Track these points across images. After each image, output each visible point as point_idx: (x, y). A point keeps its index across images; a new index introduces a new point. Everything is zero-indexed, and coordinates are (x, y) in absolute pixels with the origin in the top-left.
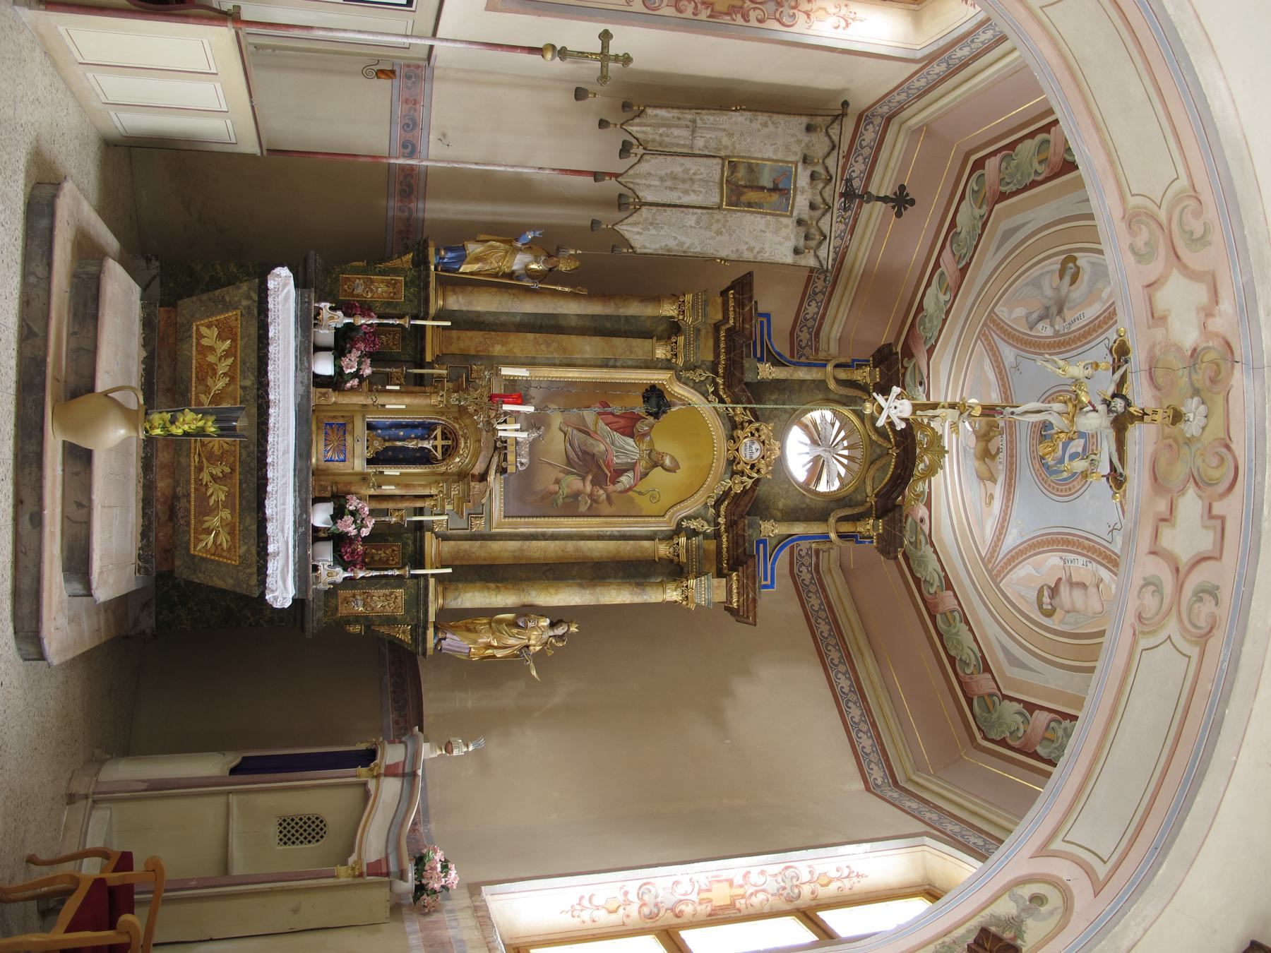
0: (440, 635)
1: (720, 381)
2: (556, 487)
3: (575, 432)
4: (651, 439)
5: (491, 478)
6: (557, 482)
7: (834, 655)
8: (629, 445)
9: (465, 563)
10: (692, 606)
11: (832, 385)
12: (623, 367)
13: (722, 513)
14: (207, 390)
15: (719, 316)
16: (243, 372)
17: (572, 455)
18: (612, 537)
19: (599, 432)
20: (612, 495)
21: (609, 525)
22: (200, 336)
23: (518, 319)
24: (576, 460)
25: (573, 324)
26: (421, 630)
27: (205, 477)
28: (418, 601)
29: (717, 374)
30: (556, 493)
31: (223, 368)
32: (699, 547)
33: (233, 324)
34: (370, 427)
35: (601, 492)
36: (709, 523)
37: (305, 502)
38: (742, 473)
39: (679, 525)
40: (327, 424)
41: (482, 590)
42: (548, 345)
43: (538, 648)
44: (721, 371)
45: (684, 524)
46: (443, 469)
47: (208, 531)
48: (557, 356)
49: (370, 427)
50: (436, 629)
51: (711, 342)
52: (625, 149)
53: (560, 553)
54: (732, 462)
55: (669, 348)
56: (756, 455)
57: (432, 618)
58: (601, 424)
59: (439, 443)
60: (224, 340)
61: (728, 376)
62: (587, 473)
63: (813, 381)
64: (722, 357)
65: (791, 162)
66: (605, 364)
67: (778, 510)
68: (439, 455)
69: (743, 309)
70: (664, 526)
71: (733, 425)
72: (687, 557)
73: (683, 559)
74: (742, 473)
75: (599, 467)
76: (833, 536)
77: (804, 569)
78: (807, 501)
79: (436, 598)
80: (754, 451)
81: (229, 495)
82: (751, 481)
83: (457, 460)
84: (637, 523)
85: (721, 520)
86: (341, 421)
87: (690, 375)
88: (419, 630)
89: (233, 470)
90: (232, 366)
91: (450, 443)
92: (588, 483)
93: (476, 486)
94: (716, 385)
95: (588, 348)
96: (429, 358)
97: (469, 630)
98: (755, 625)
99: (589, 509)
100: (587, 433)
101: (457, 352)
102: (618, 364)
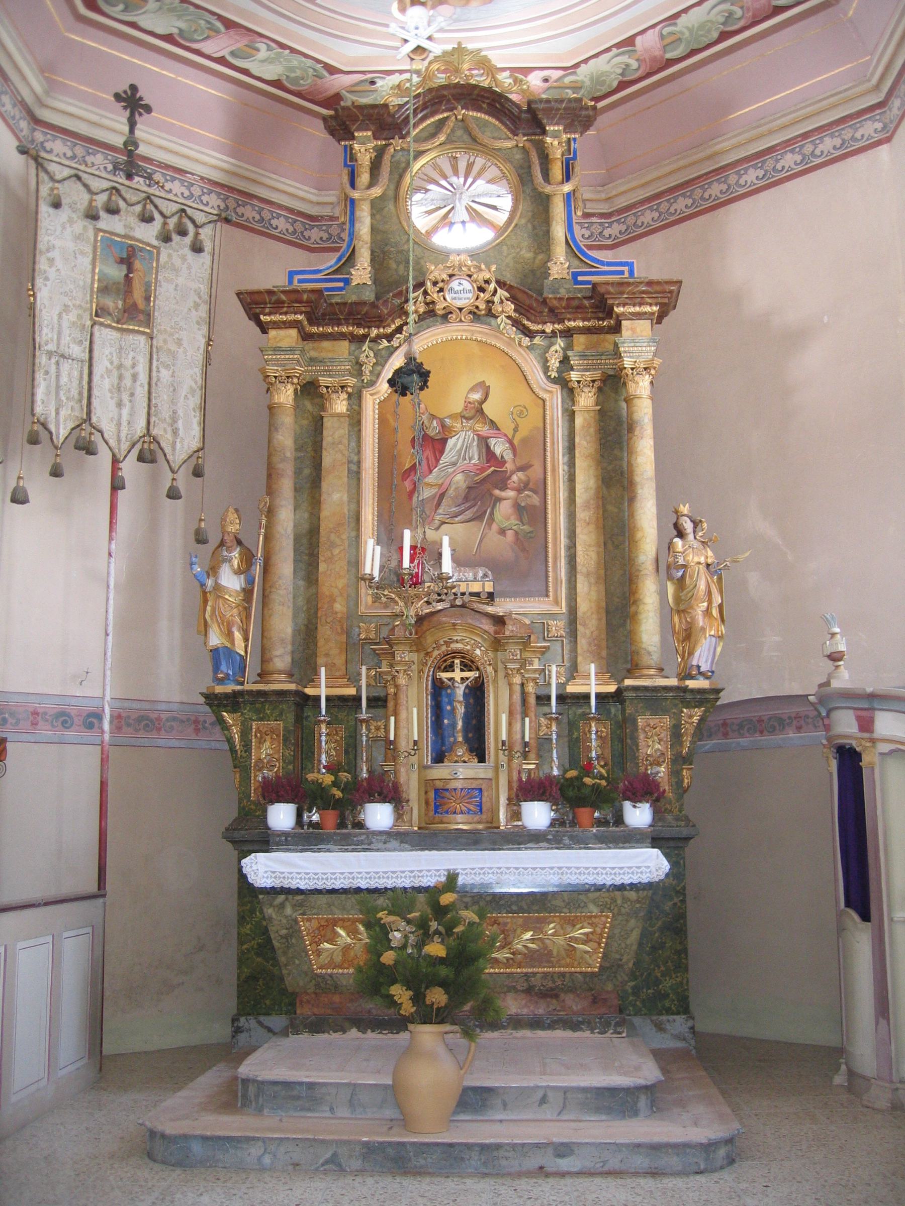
1: (374, 332)
2: (510, 533)
3: (440, 511)
4: (450, 417)
6: (502, 532)
7: (716, 190)
8: (455, 445)
9: (604, 643)
10: (657, 362)
11: (377, 191)
12: (359, 452)
13: (540, 327)
15: (293, 332)
17: (469, 514)
18: (571, 464)
19: (440, 482)
20: (518, 465)
23: (301, 583)
24: (475, 509)
25: (306, 515)
26: (689, 696)
29: (365, 336)
30: (516, 533)
32: (583, 356)
33: (315, 924)
34: (439, 758)
35: (515, 478)
36: (552, 344)
38: (490, 302)
39: (555, 381)
40: (436, 812)
42: (333, 545)
43: (710, 553)
44: (362, 331)
45: (554, 374)
46: (490, 669)
48: (347, 534)
51: (326, 344)
53: (592, 527)
54: (475, 315)
55: (334, 396)
56: (467, 285)
57: (673, 682)
58: (431, 479)
59: (457, 675)
62: (491, 495)
63: (373, 216)
64: (344, 329)
65: (96, 236)
66: (356, 475)
67: (535, 258)
69: (283, 302)
70: (555, 398)
71: (430, 314)
72: (595, 370)
73: (597, 375)
74: (490, 302)
75: (484, 480)
76: (567, 188)
78: (523, 221)
79: (650, 677)
80: (461, 288)
82: (499, 290)
83: (478, 652)
84: (552, 433)
85: (549, 328)
86: (432, 795)
87: (367, 369)
91: (457, 661)
92: (503, 494)
93: (510, 629)
94: (379, 337)
95: (336, 496)
96: (352, 691)
98: (680, 282)
99: (535, 492)
100: (442, 495)
101: (344, 657)
102: (355, 459)
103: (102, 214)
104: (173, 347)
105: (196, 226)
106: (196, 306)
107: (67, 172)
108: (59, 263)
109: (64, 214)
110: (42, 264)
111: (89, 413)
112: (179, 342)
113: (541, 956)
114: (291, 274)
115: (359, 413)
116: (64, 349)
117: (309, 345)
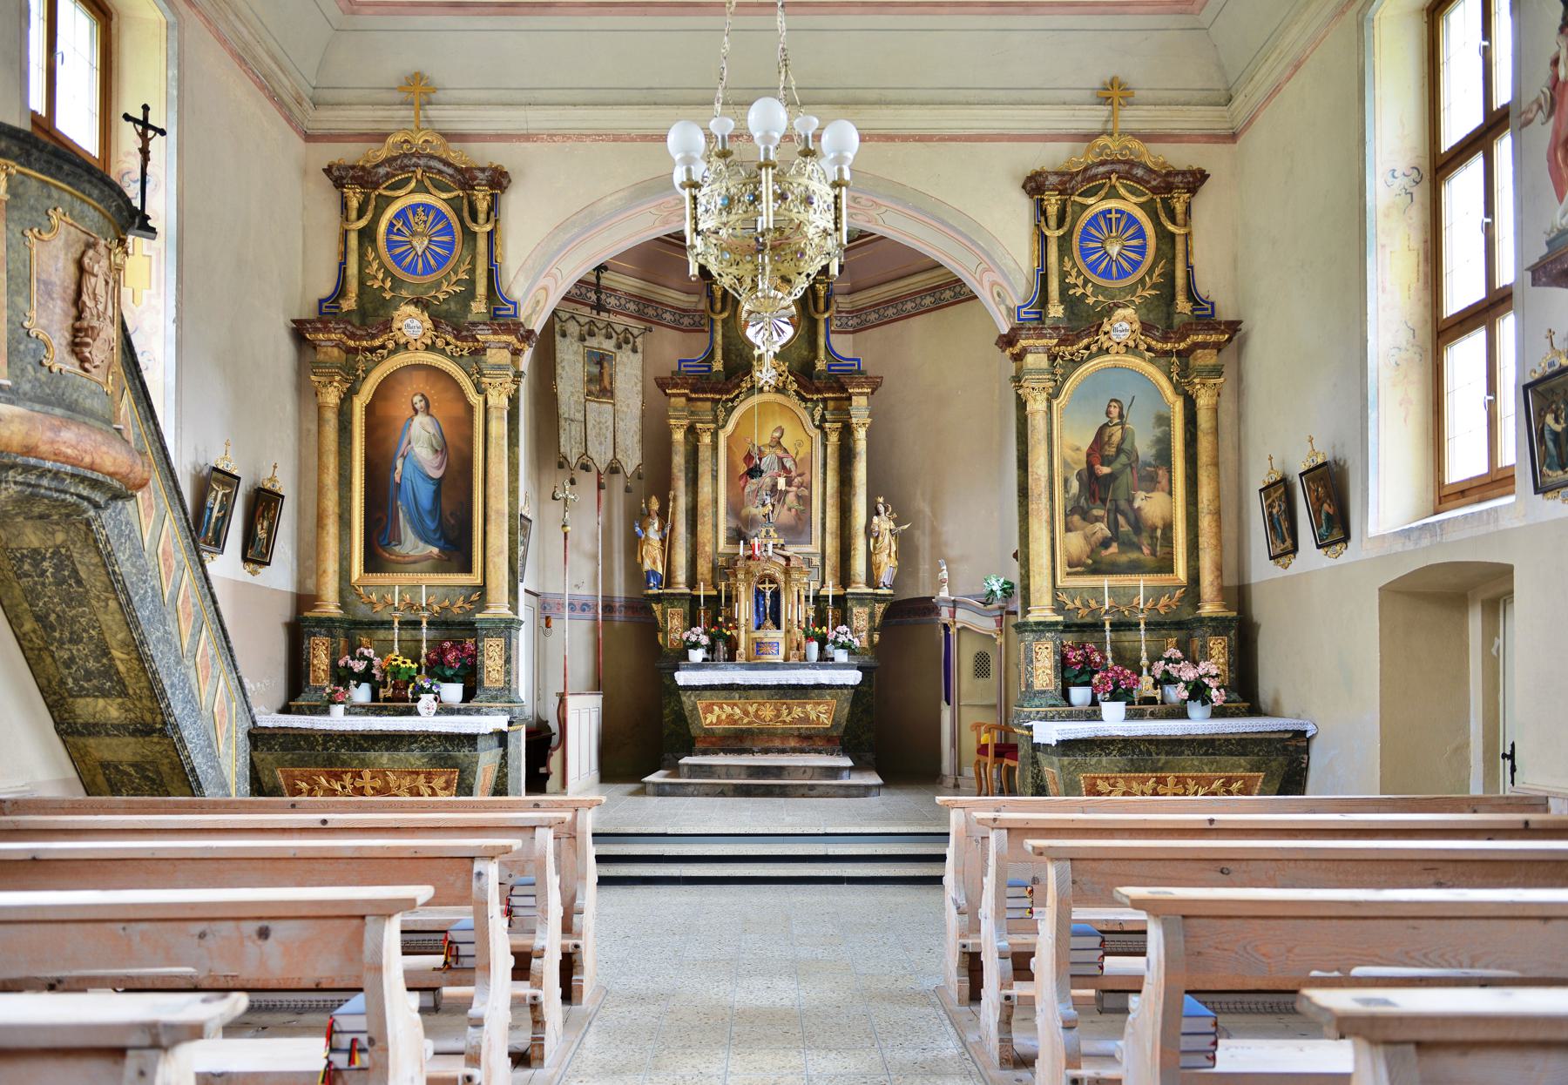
16: (731, 699)
22: (711, 723)
27: (788, 719)
31: (728, 709)
33: (704, 705)
37: (804, 663)
52: (586, 468)
60: (713, 710)
81: (799, 705)
89: (785, 703)
90: (728, 705)
94: (728, 400)
103: (587, 337)
104: (625, 409)
105: (635, 337)
106: (636, 384)
107: (568, 315)
108: (567, 368)
109: (568, 340)
110: (559, 370)
111: (586, 450)
112: (628, 406)
113: (806, 719)
117: (691, 404)
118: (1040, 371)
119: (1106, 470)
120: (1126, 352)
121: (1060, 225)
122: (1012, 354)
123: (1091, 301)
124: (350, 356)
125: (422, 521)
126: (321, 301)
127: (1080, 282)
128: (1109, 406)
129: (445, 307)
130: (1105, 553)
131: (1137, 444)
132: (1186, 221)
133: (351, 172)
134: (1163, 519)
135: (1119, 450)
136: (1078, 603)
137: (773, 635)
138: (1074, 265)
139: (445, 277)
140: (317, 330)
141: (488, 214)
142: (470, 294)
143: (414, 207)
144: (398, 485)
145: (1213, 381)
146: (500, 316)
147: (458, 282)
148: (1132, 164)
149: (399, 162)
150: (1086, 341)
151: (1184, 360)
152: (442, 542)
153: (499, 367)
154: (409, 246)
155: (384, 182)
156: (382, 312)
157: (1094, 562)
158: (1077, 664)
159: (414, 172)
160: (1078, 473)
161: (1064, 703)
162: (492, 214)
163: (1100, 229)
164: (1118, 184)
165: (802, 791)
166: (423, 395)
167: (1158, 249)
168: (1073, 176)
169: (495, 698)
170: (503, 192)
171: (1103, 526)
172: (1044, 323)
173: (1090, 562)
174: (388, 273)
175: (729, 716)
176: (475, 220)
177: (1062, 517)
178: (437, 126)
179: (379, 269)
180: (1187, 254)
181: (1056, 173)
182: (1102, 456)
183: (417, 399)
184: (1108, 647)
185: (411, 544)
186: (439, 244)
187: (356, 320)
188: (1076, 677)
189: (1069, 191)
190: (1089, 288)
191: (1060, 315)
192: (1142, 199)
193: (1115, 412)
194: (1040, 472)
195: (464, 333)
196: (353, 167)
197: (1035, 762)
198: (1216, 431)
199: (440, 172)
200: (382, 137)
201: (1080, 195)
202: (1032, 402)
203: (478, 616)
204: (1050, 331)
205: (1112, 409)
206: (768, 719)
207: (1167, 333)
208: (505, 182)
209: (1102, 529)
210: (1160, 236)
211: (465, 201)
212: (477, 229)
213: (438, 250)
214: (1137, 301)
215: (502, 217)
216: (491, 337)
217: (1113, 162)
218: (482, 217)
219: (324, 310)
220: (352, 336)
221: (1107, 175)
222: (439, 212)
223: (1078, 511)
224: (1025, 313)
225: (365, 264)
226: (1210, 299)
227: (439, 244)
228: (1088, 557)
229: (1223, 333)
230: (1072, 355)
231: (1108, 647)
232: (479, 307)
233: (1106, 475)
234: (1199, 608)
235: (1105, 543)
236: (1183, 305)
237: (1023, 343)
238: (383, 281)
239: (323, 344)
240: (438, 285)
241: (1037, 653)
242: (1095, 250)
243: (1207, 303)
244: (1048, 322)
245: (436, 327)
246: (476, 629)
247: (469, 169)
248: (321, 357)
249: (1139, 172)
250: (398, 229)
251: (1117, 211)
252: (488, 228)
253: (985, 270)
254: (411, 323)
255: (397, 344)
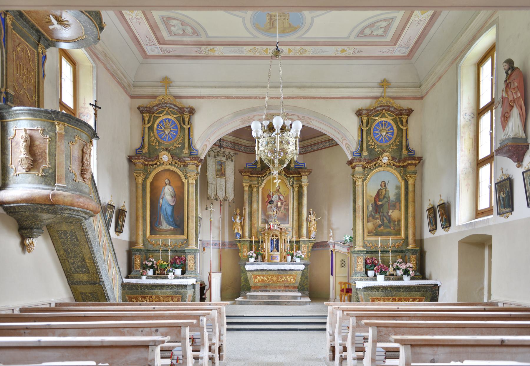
0: (311, 237)
5: (281, 227)
6: (282, 213)
14: (266, 280)
21: (291, 202)
22: (257, 282)
27: (281, 281)
28: (304, 242)
31: (262, 277)
32: (296, 182)
34: (272, 251)
37: (286, 262)
41: (303, 229)
45: (291, 184)
47: (291, 280)
49: (272, 251)
50: (310, 238)
53: (296, 212)
57: (308, 239)
59: (275, 238)
61: (260, 174)
68: (277, 238)
73: (298, 185)
77: (302, 151)
81: (284, 276)
88: (310, 242)
90: (262, 276)
93: (283, 230)
96: (258, 240)
97: (311, 232)
114: (247, 164)
115: (258, 191)
116: (212, 183)
118: (360, 172)
119: (380, 203)
120: (387, 166)
121: (367, 126)
122: (352, 167)
123: (376, 150)
124: (146, 167)
125: (168, 219)
126: (136, 150)
127: (373, 144)
128: (381, 183)
129: (175, 151)
130: (379, 229)
131: (390, 195)
132: (406, 125)
133: (146, 109)
134: (398, 218)
135: (384, 197)
136: (371, 245)
137: (276, 253)
138: (371, 138)
139: (175, 142)
140: (136, 159)
141: (189, 122)
142: (183, 147)
143: (165, 120)
144: (161, 208)
145: (413, 176)
146: (192, 154)
147: (179, 144)
148: (389, 106)
149: (161, 105)
150: (374, 163)
151: (405, 168)
152: (174, 226)
153: (192, 171)
154: (164, 132)
155: (156, 112)
156: (155, 153)
157: (376, 232)
158: (370, 264)
159: (165, 108)
160: (372, 204)
161: (366, 275)
162: (190, 122)
163: (379, 127)
164: (385, 113)
165: (285, 303)
166: (168, 179)
167: (397, 133)
168: (371, 110)
169: (191, 274)
170: (193, 115)
171: (379, 221)
172: (361, 157)
173: (375, 232)
174: (157, 140)
175: (262, 280)
176: (184, 124)
177: (366, 218)
178: (172, 94)
179: (154, 139)
180: (406, 135)
181: (366, 110)
182: (379, 199)
183: (166, 180)
184: (380, 258)
185: (165, 226)
186: (173, 131)
187: (148, 156)
188: (370, 267)
189: (370, 115)
190: (376, 146)
191: (367, 155)
192: (393, 118)
193: (383, 185)
194: (359, 204)
195: (181, 160)
196: (146, 107)
197: (357, 294)
198: (414, 191)
199: (173, 109)
200: (155, 97)
201: (373, 116)
202: (357, 182)
203: (186, 248)
204: (363, 160)
205: (382, 184)
206: (275, 280)
207: (400, 160)
208: (194, 112)
209: (379, 222)
210: (398, 129)
211: (181, 118)
212: (185, 127)
213: (173, 133)
214: (391, 150)
215: (193, 123)
216: (190, 161)
217: (384, 106)
218: (187, 123)
219: (137, 152)
220: (147, 161)
221: (382, 110)
222: (173, 121)
223: (371, 217)
224: (356, 154)
225: (150, 138)
226: (413, 150)
227: (173, 131)
228: (374, 230)
229: (417, 160)
230: (370, 167)
231: (380, 258)
232: (186, 152)
233: (380, 205)
234: (408, 246)
235: (380, 226)
236: (405, 151)
237: (355, 163)
238: (156, 143)
239: (137, 163)
240: (173, 145)
241: (358, 260)
242: (378, 134)
243: (412, 151)
244: (363, 157)
245: (172, 158)
246: (185, 252)
247: (183, 108)
248: (137, 167)
249: (392, 109)
250: (160, 127)
251: (385, 121)
252: (189, 126)
253: (344, 140)
254: (165, 157)
255: (160, 163)
